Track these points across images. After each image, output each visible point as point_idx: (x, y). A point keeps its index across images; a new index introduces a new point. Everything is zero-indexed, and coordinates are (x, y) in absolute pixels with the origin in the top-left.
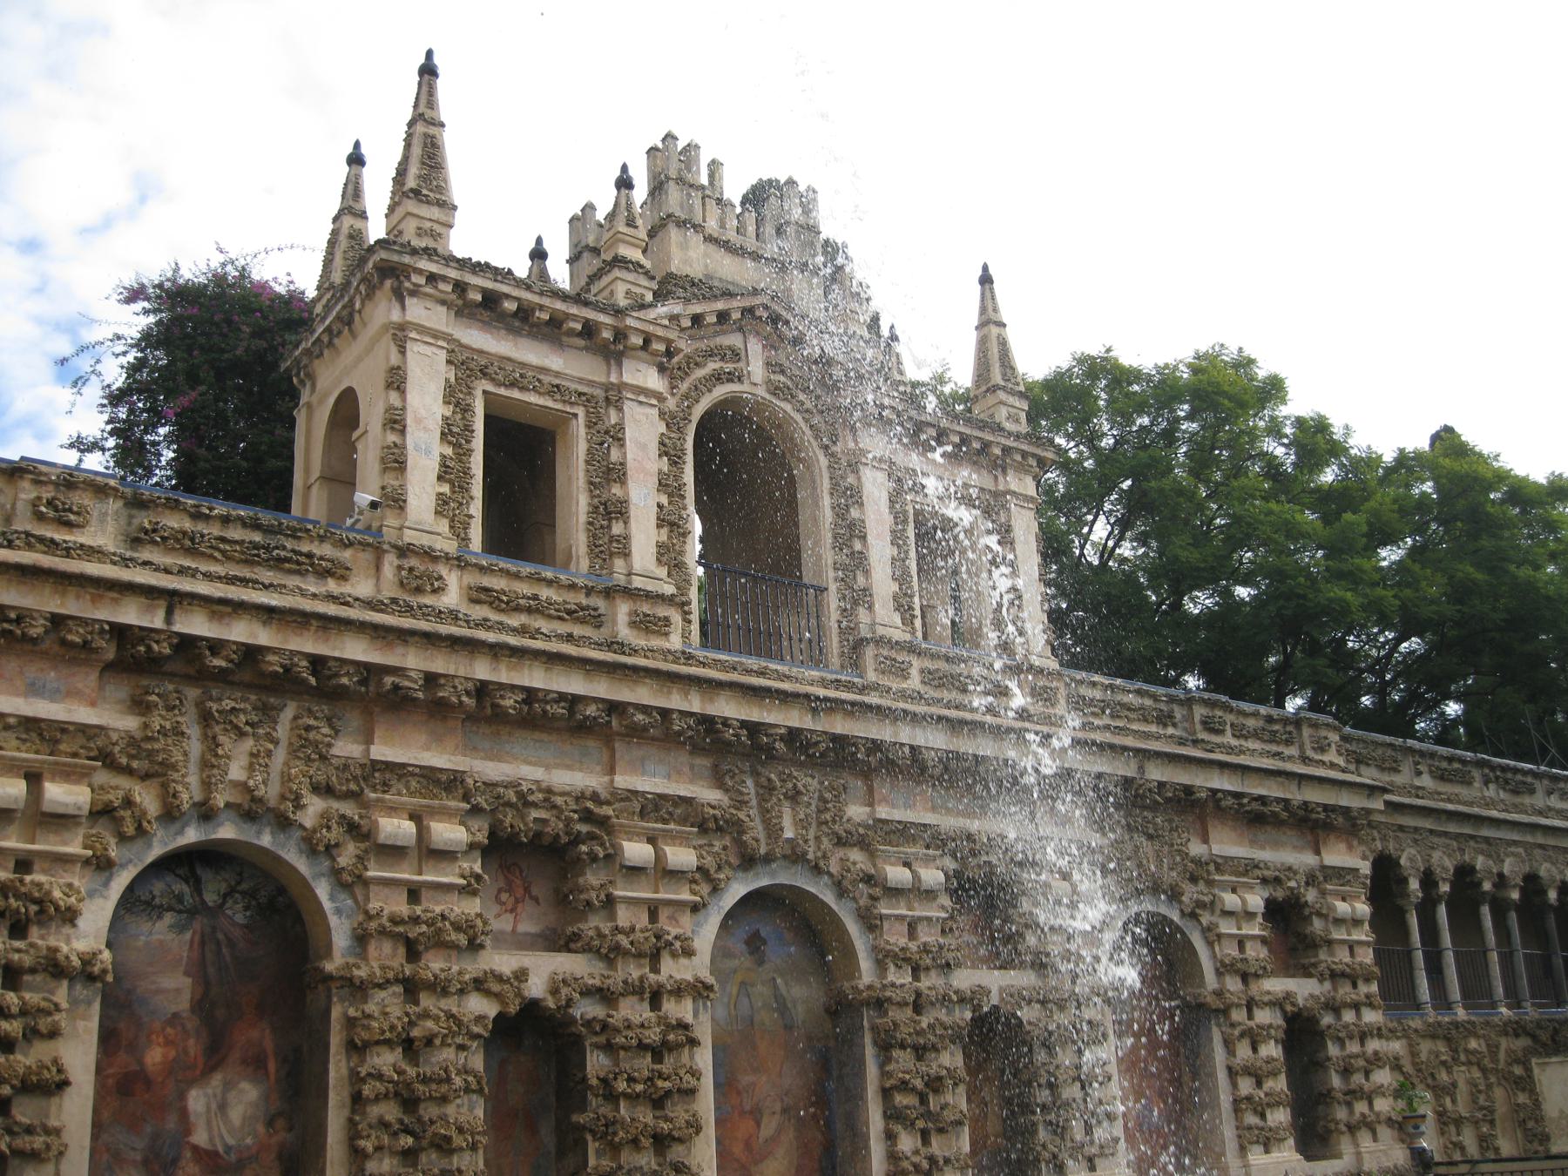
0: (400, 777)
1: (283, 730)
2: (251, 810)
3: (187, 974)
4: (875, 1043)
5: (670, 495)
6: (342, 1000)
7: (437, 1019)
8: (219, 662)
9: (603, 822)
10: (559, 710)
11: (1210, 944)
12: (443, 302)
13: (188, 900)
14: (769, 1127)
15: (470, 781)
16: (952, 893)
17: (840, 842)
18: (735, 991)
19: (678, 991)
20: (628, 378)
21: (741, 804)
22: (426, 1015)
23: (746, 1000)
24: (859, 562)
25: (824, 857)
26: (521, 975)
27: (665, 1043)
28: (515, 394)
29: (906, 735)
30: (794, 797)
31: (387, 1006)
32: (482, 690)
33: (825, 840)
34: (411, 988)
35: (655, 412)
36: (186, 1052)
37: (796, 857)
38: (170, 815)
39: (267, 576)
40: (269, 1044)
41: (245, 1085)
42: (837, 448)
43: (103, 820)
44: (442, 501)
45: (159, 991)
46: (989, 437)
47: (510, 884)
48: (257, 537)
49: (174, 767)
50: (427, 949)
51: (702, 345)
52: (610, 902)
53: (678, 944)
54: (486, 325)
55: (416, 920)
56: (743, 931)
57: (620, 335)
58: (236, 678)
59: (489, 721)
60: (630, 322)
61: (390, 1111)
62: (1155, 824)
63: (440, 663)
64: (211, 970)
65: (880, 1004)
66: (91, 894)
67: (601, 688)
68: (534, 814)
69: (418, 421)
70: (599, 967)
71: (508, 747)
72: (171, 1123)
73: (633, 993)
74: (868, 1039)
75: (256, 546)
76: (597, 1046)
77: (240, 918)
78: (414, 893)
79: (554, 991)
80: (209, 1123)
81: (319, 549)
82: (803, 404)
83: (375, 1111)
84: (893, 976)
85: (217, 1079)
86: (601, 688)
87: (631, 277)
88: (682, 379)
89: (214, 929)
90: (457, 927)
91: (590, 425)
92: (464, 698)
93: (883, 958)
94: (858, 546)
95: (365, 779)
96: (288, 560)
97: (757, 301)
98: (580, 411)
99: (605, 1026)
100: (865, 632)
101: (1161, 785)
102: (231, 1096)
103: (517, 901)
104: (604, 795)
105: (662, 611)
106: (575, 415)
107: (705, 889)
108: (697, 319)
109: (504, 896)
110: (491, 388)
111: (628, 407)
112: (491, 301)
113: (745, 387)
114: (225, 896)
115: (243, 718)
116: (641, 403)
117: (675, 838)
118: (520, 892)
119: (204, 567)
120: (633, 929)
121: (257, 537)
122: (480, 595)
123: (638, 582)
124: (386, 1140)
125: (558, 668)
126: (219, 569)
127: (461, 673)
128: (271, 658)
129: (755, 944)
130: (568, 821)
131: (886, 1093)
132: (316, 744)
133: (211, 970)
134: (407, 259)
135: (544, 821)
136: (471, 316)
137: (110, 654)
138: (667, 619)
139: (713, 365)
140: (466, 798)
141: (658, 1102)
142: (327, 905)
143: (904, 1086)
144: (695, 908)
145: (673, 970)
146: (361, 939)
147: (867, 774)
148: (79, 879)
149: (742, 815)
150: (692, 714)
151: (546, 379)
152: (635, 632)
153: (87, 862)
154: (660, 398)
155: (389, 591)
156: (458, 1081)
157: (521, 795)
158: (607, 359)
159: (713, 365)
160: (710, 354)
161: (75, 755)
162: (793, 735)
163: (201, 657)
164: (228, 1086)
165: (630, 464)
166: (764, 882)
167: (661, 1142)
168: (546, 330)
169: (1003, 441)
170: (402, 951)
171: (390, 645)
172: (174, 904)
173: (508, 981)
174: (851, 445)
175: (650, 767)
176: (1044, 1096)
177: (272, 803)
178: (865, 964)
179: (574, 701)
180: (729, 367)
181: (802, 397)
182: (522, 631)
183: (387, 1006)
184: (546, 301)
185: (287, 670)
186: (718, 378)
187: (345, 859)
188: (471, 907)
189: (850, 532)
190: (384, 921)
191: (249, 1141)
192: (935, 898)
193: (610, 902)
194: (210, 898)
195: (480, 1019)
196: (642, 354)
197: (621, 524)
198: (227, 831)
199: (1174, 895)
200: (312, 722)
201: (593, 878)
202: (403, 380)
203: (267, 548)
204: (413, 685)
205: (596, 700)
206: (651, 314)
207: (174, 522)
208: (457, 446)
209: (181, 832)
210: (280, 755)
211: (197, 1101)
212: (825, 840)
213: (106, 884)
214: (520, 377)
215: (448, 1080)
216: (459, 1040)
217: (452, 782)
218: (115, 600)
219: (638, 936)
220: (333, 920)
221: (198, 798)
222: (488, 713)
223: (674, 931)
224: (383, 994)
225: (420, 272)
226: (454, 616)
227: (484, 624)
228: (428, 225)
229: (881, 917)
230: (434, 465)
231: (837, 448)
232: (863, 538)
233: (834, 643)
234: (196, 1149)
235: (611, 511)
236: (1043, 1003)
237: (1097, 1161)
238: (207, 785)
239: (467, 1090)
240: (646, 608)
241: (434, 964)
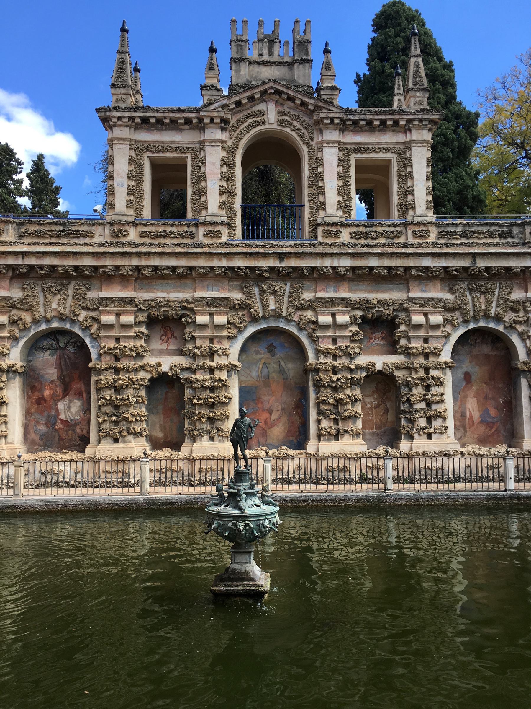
0: (113, 302)
1: (70, 292)
2: (62, 318)
3: (55, 368)
4: (315, 385)
5: (227, 180)
6: (95, 375)
7: (123, 380)
8: (43, 272)
9: (191, 309)
10: (168, 272)
11: (523, 340)
12: (127, 126)
13: (55, 346)
14: (274, 416)
15: (137, 300)
16: (360, 326)
17: (298, 309)
18: (261, 366)
19: (220, 368)
20: (206, 138)
21: (250, 297)
22: (119, 379)
23: (266, 370)
24: (321, 191)
25: (290, 315)
26: (159, 364)
27: (213, 386)
28: (161, 155)
29: (328, 263)
30: (275, 293)
31: (109, 377)
32: (137, 269)
33: (290, 308)
34: (117, 371)
35: (220, 147)
36: (57, 392)
37: (278, 316)
38: (36, 322)
39: (64, 240)
40: (83, 389)
41: (76, 401)
42: (313, 143)
43: (15, 325)
44: (129, 204)
45: (47, 374)
46: (396, 117)
47: (165, 333)
48: (61, 228)
49: (33, 307)
50: (122, 357)
51: (245, 113)
52: (193, 338)
53: (220, 351)
55: (116, 348)
56: (265, 345)
57: (201, 120)
58: (54, 276)
59: (141, 279)
60: (202, 114)
61: (108, 409)
62: (486, 287)
63: (119, 262)
64: (63, 367)
65: (317, 371)
66: (12, 347)
67: (183, 262)
68: (163, 309)
69: (118, 175)
70: (190, 360)
71: (155, 287)
72: (53, 412)
73: (201, 369)
74: (311, 384)
75: (60, 231)
76: (189, 387)
77: (71, 350)
78: (118, 339)
79: (171, 369)
80: (65, 412)
81: (82, 228)
82: (295, 127)
83: (104, 409)
84: (322, 360)
85: (66, 400)
86: (183, 262)
87: (209, 93)
88: (235, 131)
89: (63, 354)
90: (132, 350)
91: (193, 160)
92: (131, 273)
93: (318, 352)
94: (320, 184)
95: (99, 304)
96: (71, 234)
97: (267, 86)
98: (189, 155)
99: (191, 382)
100: (319, 220)
101: (488, 269)
102: (72, 404)
103: (168, 339)
104: (190, 300)
105: (217, 228)
107: (235, 331)
108: (238, 103)
109: (163, 337)
110: (151, 154)
111: (207, 148)
112: (145, 120)
113: (267, 126)
114: (66, 344)
115: (54, 289)
116: (213, 146)
117: (220, 313)
118: (170, 336)
119: (41, 241)
120: (201, 347)
121: (61, 228)
122: (143, 234)
123: (208, 219)
124: (106, 418)
125: (165, 257)
126: (47, 241)
127: (127, 264)
128: (59, 268)
129: (271, 349)
130: (176, 310)
131: (318, 404)
132: (80, 294)
133: (63, 367)
134: (108, 113)
135: (168, 311)
136: (141, 128)
137: (10, 274)
138: (219, 231)
139: (250, 121)
140: (136, 306)
141: (212, 406)
142: (89, 345)
143: (324, 402)
144: (229, 338)
145: (218, 360)
146: (100, 355)
147: (315, 280)
148: (7, 344)
149: (250, 302)
150: (224, 267)
151: (173, 146)
152: (206, 238)
153: (9, 338)
154: (222, 141)
155: (109, 239)
156: (132, 400)
157: (157, 303)
158: (200, 130)
159: (250, 121)
160: (249, 116)
161: (4, 306)
162: (272, 269)
163: (37, 272)
164: (70, 401)
165: (208, 171)
166: (264, 326)
167: (211, 420)
168: (172, 126)
169: (405, 117)
170: (113, 358)
171: (99, 258)
172: (51, 348)
173: (153, 366)
174: (320, 139)
175: (211, 288)
176: (404, 407)
177: (68, 314)
178: (311, 355)
179: (174, 269)
180: (258, 119)
181: (295, 123)
182: (159, 245)
183: (109, 377)
184: (166, 115)
185: (66, 272)
186: (252, 126)
187: (92, 331)
188: (140, 343)
189: (317, 178)
190: (106, 349)
191: (78, 417)
192: (348, 328)
193: (193, 338)
194: (62, 345)
195: (142, 379)
196: (211, 125)
197: (205, 197)
198: (55, 325)
199: (498, 319)
200: (77, 287)
201: (188, 330)
203: (63, 231)
204: (110, 271)
205: (182, 267)
206: (212, 107)
207: (32, 228)
208: (135, 180)
209: (40, 326)
210: (70, 300)
211: (61, 406)
212: (290, 308)
213: (17, 344)
214: (163, 147)
215: (128, 399)
216: (135, 386)
217: (131, 301)
218: (5, 258)
219: (202, 350)
220: (91, 350)
221: (43, 315)
222: (140, 277)
223: (219, 347)
224: (107, 372)
225: (114, 117)
226: (130, 244)
227: (144, 245)
228: (120, 96)
229: (317, 337)
230: (125, 190)
231: (313, 143)
232: (323, 180)
233: (307, 228)
234: (61, 420)
235: (201, 192)
236: (407, 368)
237: (433, 436)
238: (45, 311)
239: (137, 402)
240: (211, 228)
241: (124, 363)
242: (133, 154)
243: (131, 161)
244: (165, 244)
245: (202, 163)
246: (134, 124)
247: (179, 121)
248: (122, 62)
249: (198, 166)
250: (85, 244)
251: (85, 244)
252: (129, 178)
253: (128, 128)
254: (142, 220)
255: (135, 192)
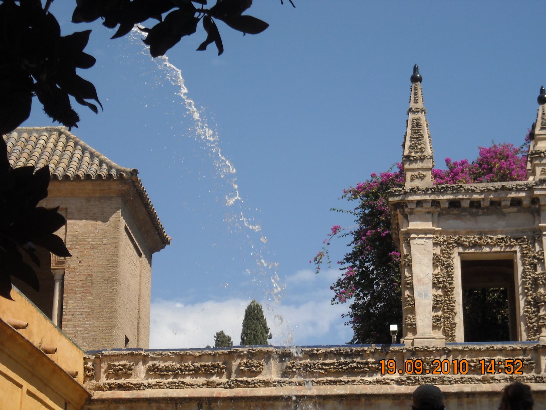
12: (429, 213)
44: (437, 319)
54: (458, 217)
60: (537, 193)
69: (419, 281)
91: (524, 256)
96: (357, 367)
106: (515, 252)
182: (484, 380)
202: (410, 261)
228: (416, 173)
230: (429, 302)
242: (438, 250)
243: (436, 261)
244: (492, 379)
245: (538, 259)
246: (439, 209)
247: (503, 203)
248: (418, 125)
249: (532, 264)
250: (378, 382)
251: (378, 382)
252: (434, 284)
253: (430, 215)
254: (456, 344)
255: (442, 305)
